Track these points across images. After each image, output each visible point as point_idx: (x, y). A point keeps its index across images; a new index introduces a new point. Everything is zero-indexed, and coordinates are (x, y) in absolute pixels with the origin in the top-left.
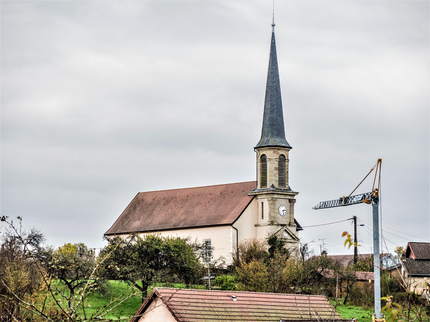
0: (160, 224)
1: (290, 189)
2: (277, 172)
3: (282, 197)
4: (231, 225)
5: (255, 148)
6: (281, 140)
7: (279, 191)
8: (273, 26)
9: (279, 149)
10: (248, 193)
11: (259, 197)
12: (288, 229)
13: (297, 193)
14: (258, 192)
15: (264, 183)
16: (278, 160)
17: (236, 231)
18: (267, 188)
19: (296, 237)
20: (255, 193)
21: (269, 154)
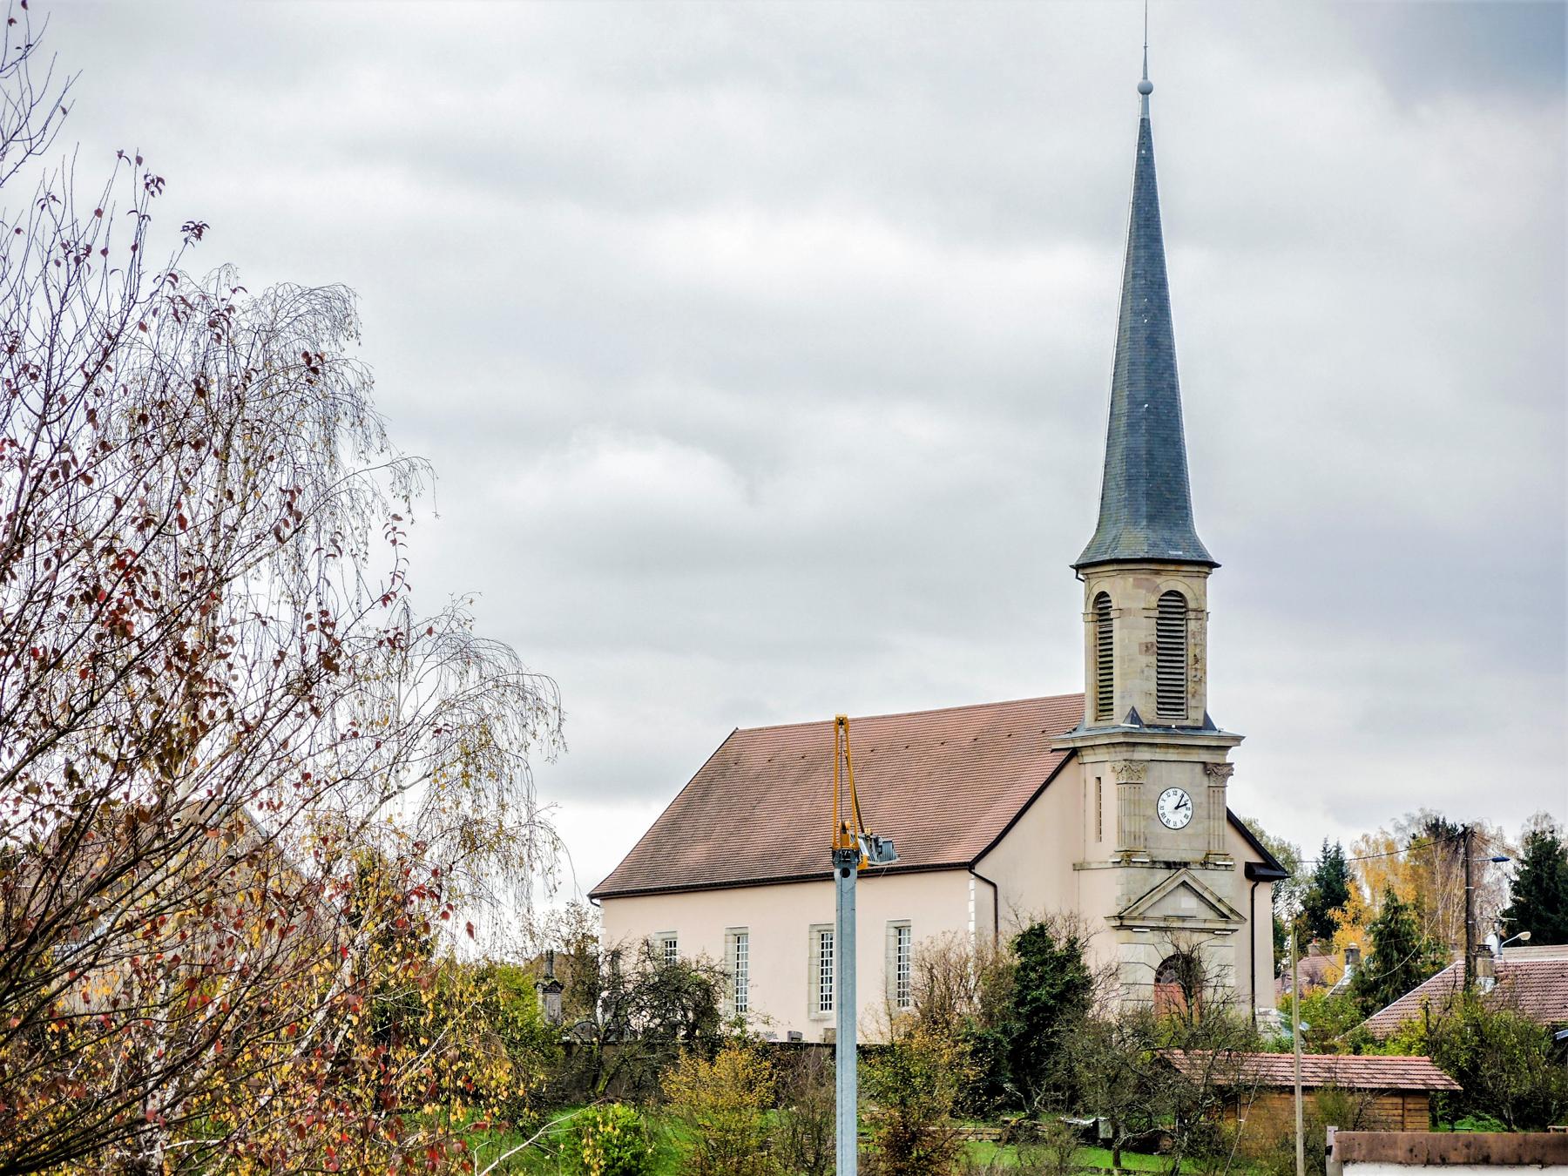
0: (762, 858)
1: (1208, 724)
2: (1153, 659)
3: (1172, 755)
4: (969, 866)
5: (1078, 568)
6: (1167, 534)
7: (1154, 735)
8: (1146, 91)
9: (1158, 572)
10: (1051, 742)
11: (1088, 757)
12: (1195, 880)
13: (1238, 739)
14: (1083, 738)
15: (1104, 705)
16: (1156, 614)
17: (990, 889)
18: (1114, 722)
19: (1231, 910)
20: (1073, 740)
21: (1125, 591)
